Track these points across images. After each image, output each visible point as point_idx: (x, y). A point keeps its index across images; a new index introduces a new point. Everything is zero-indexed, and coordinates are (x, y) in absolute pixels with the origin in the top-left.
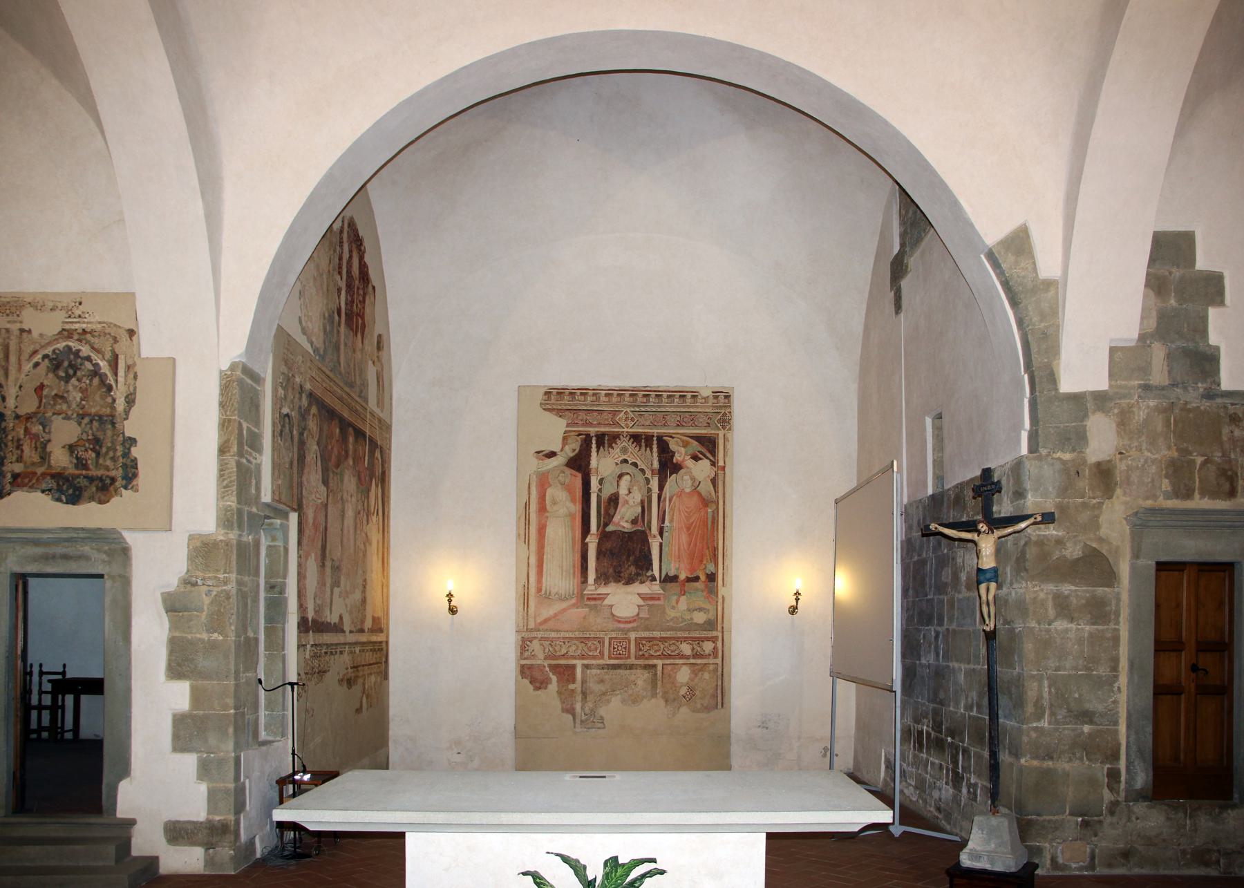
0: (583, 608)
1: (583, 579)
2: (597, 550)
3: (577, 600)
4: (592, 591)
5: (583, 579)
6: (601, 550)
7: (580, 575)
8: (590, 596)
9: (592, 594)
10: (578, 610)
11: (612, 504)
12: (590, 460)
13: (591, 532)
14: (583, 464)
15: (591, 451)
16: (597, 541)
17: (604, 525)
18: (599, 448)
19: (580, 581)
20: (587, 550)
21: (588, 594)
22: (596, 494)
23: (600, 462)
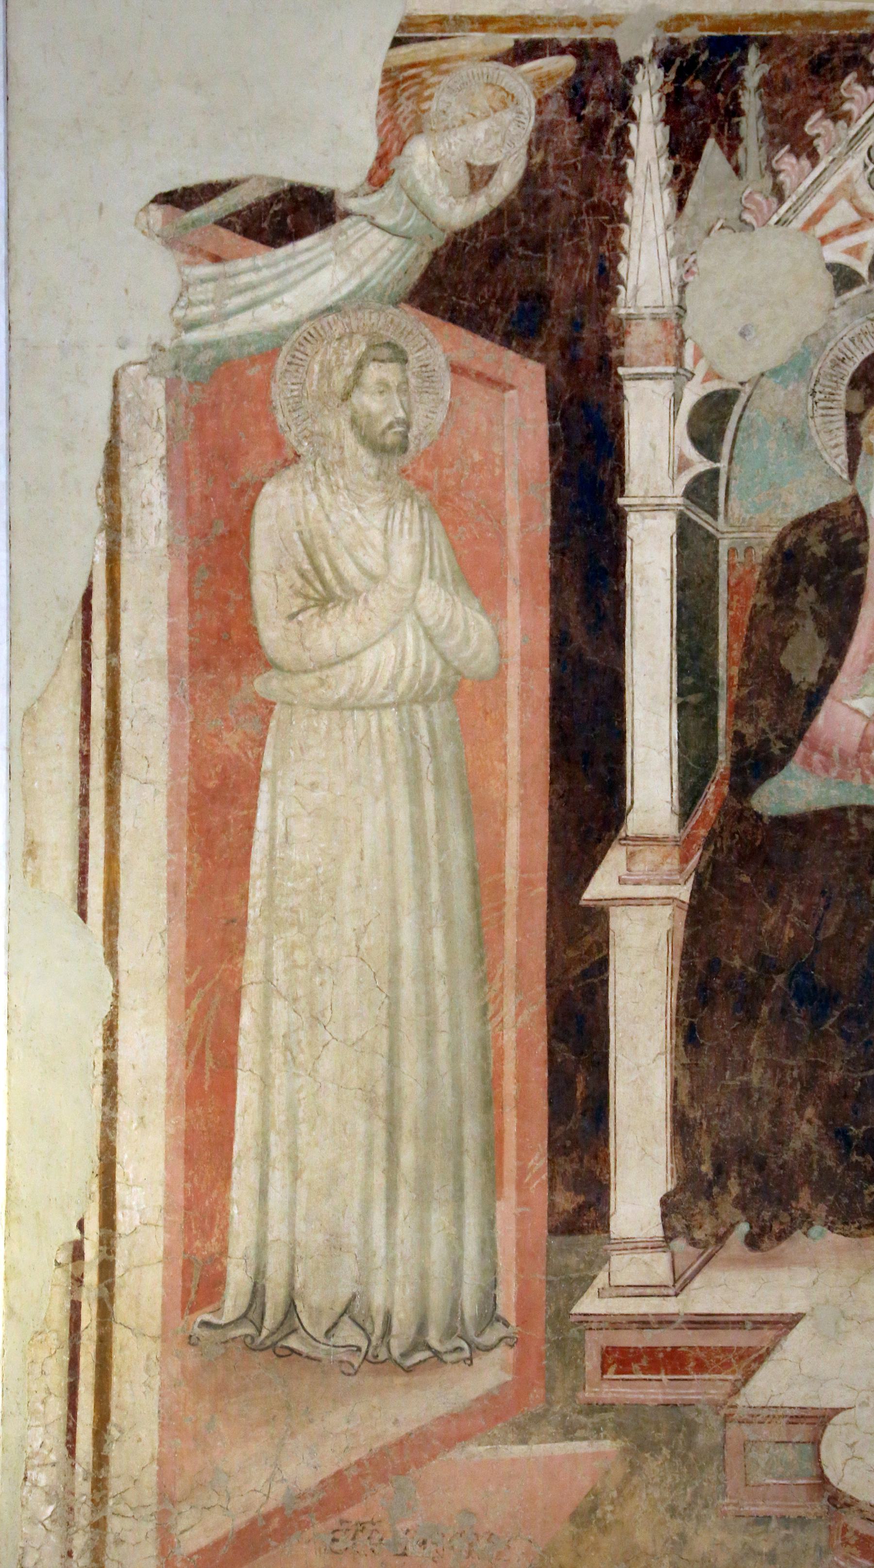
0: (568, 1433)
1: (567, 1201)
2: (687, 968)
3: (519, 1367)
4: (641, 1291)
5: (567, 1201)
6: (713, 966)
7: (539, 1161)
8: (630, 1339)
9: (643, 1323)
10: (539, 1449)
11: (807, 596)
12: (616, 251)
13: (634, 824)
14: (560, 286)
15: (622, 182)
16: (684, 892)
17: (737, 768)
18: (696, 155)
19: (541, 1222)
20: (603, 964)
21: (616, 1323)
22: (668, 524)
23: (704, 262)
